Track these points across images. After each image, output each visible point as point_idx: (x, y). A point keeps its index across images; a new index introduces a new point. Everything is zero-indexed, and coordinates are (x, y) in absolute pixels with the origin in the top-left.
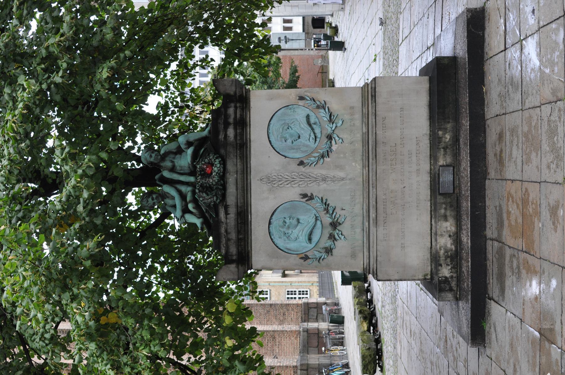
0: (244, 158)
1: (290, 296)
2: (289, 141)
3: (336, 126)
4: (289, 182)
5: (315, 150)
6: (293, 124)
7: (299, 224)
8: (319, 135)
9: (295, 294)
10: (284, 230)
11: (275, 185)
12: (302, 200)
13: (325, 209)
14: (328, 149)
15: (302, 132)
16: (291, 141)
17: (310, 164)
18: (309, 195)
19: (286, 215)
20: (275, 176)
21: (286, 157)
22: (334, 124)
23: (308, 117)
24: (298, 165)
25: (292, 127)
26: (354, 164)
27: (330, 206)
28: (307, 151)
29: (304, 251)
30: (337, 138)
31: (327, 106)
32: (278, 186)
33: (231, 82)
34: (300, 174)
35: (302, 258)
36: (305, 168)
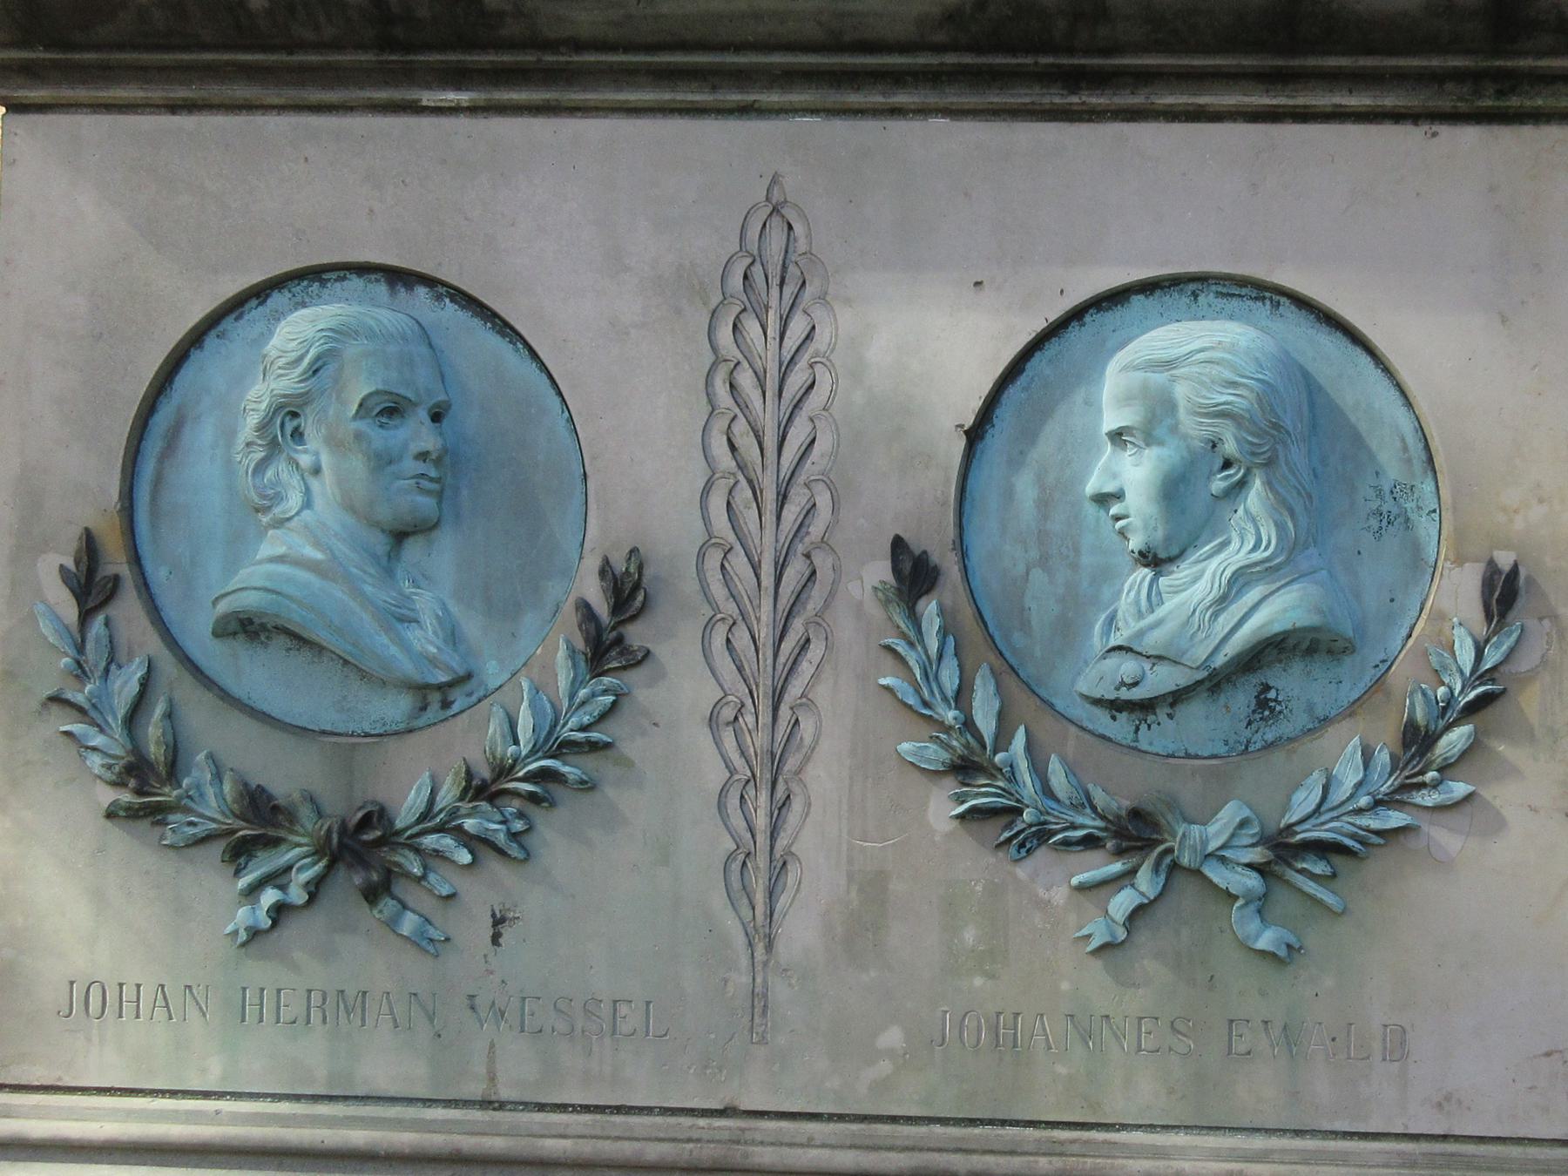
0: (975, 48)
8: (1161, 735)
12: (592, 563)
13: (504, 770)
17: (902, 648)
18: (636, 635)
20: (809, 337)
21: (975, 434)
22: (1253, 881)
24: (898, 544)
26: (892, 1037)
27: (532, 810)
29: (158, 574)
31: (1424, 822)
34: (822, 561)
36: (874, 610)
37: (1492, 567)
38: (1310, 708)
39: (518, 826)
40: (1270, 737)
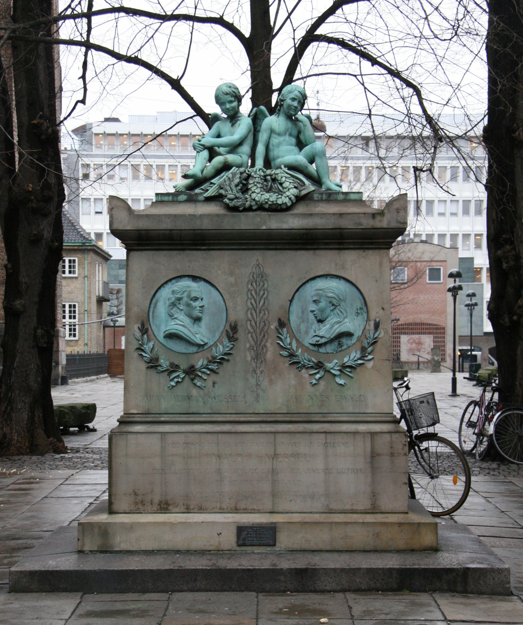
1: (67, 309)
2: (313, 307)
3: (335, 375)
4: (255, 305)
5: (300, 344)
6: (339, 312)
7: (193, 321)
8: (322, 350)
9: (70, 317)
10: (185, 299)
11: (250, 286)
13: (214, 358)
14: (302, 363)
15: (328, 326)
16: (314, 309)
17: (280, 336)
18: (235, 336)
19: (204, 303)
23: (349, 335)
24: (280, 320)
25: (335, 311)
27: (220, 366)
28: (300, 332)
30: (318, 376)
32: (249, 290)
33: (402, 221)
35: (143, 325)
37: (375, 320)
38: (347, 344)
39: (217, 367)
40: (341, 349)
